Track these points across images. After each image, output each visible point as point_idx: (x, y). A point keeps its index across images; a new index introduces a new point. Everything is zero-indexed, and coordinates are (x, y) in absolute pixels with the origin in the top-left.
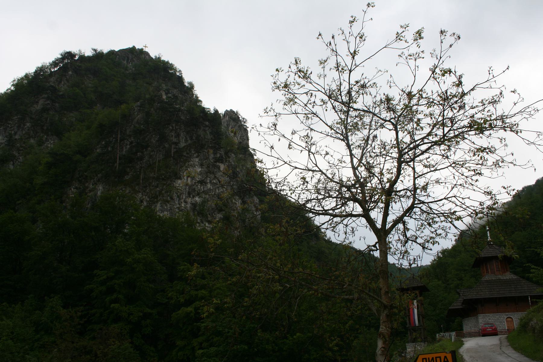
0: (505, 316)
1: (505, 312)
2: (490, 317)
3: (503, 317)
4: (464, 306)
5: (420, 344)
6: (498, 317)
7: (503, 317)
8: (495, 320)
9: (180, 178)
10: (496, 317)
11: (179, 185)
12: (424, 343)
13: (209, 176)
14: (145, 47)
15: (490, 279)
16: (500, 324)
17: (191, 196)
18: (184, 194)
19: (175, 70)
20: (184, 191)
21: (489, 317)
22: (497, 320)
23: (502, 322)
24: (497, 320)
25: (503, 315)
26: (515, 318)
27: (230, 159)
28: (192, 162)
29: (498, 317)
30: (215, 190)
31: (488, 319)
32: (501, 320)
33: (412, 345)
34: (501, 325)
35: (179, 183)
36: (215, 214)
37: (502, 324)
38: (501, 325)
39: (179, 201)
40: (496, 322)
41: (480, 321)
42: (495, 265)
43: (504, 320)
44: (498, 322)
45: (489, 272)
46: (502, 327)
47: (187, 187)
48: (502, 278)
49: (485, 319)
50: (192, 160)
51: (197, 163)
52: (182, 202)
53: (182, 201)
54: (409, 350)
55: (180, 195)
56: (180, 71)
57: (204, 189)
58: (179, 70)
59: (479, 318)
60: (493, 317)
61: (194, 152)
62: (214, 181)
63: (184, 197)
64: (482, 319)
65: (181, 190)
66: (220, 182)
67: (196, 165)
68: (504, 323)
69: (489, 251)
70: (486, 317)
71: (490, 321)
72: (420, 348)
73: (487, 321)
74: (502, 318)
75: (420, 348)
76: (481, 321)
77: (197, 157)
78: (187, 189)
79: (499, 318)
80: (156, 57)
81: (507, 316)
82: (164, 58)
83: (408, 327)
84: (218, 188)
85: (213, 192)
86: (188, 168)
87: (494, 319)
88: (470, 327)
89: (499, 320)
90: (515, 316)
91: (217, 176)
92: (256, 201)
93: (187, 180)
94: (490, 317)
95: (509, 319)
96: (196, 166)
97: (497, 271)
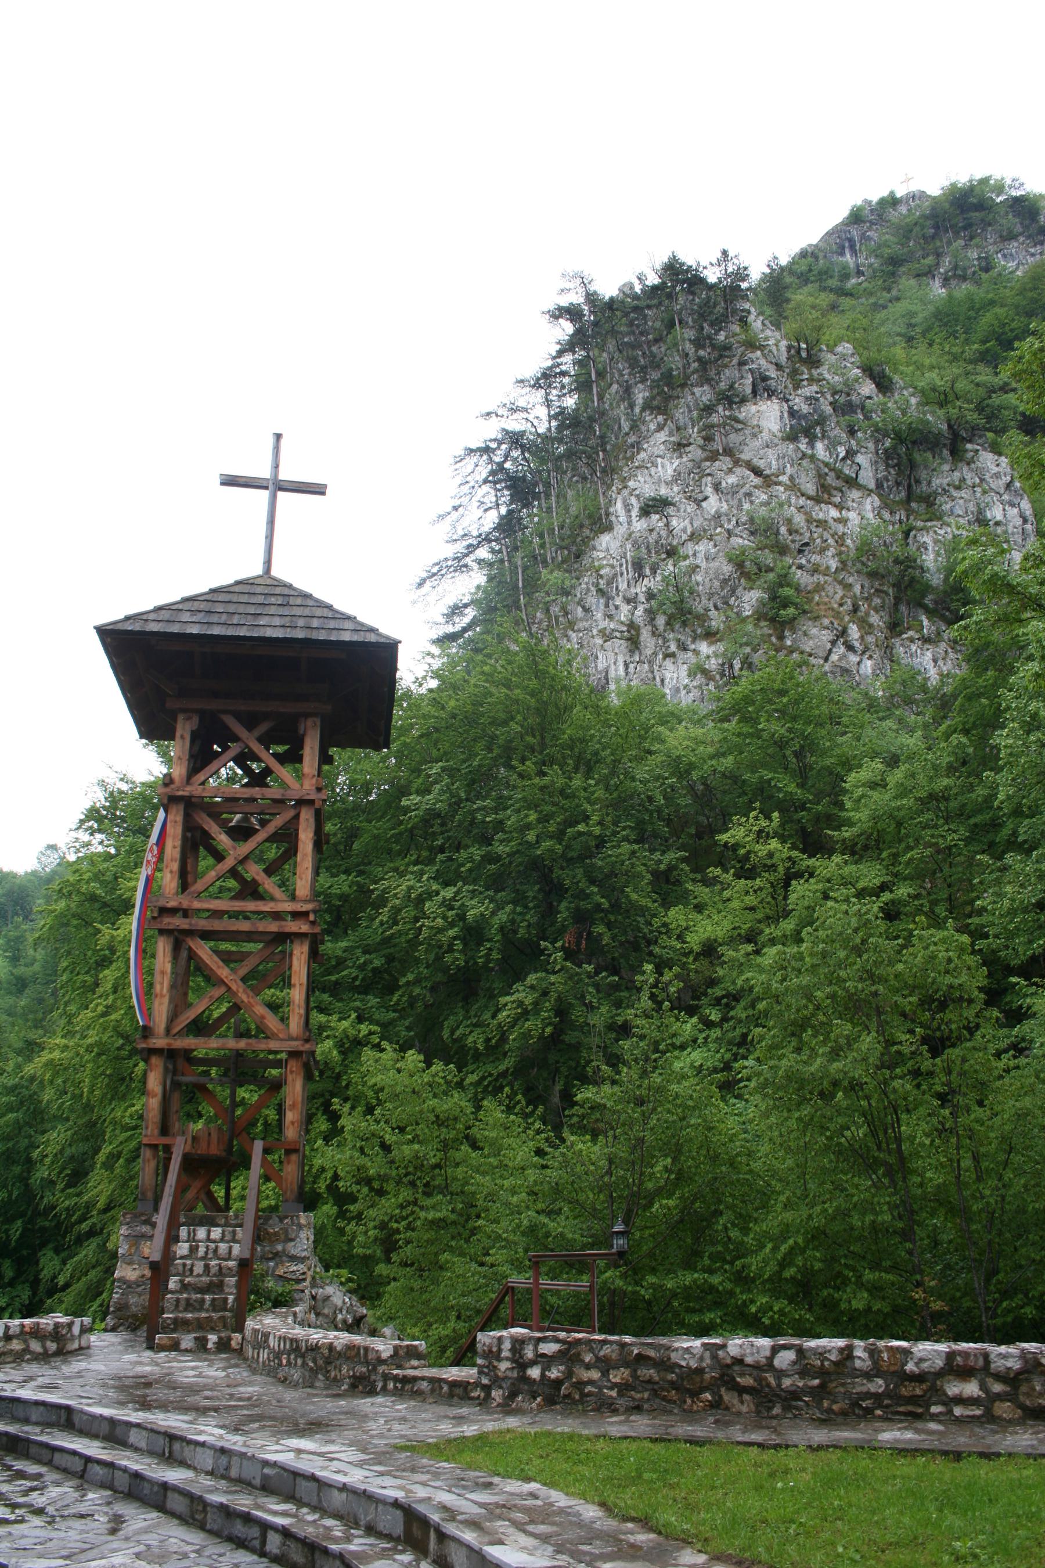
9: (609, 528)
11: (608, 550)
17: (648, 571)
18: (622, 574)
20: (621, 565)
28: (643, 455)
30: (740, 506)
35: (604, 545)
39: (607, 606)
47: (629, 546)
51: (662, 447)
52: (617, 607)
53: (618, 601)
55: (609, 583)
62: (732, 479)
63: (623, 586)
65: (613, 567)
77: (660, 428)
84: (749, 495)
85: (729, 521)
91: (744, 457)
92: (996, 469)
96: (659, 460)
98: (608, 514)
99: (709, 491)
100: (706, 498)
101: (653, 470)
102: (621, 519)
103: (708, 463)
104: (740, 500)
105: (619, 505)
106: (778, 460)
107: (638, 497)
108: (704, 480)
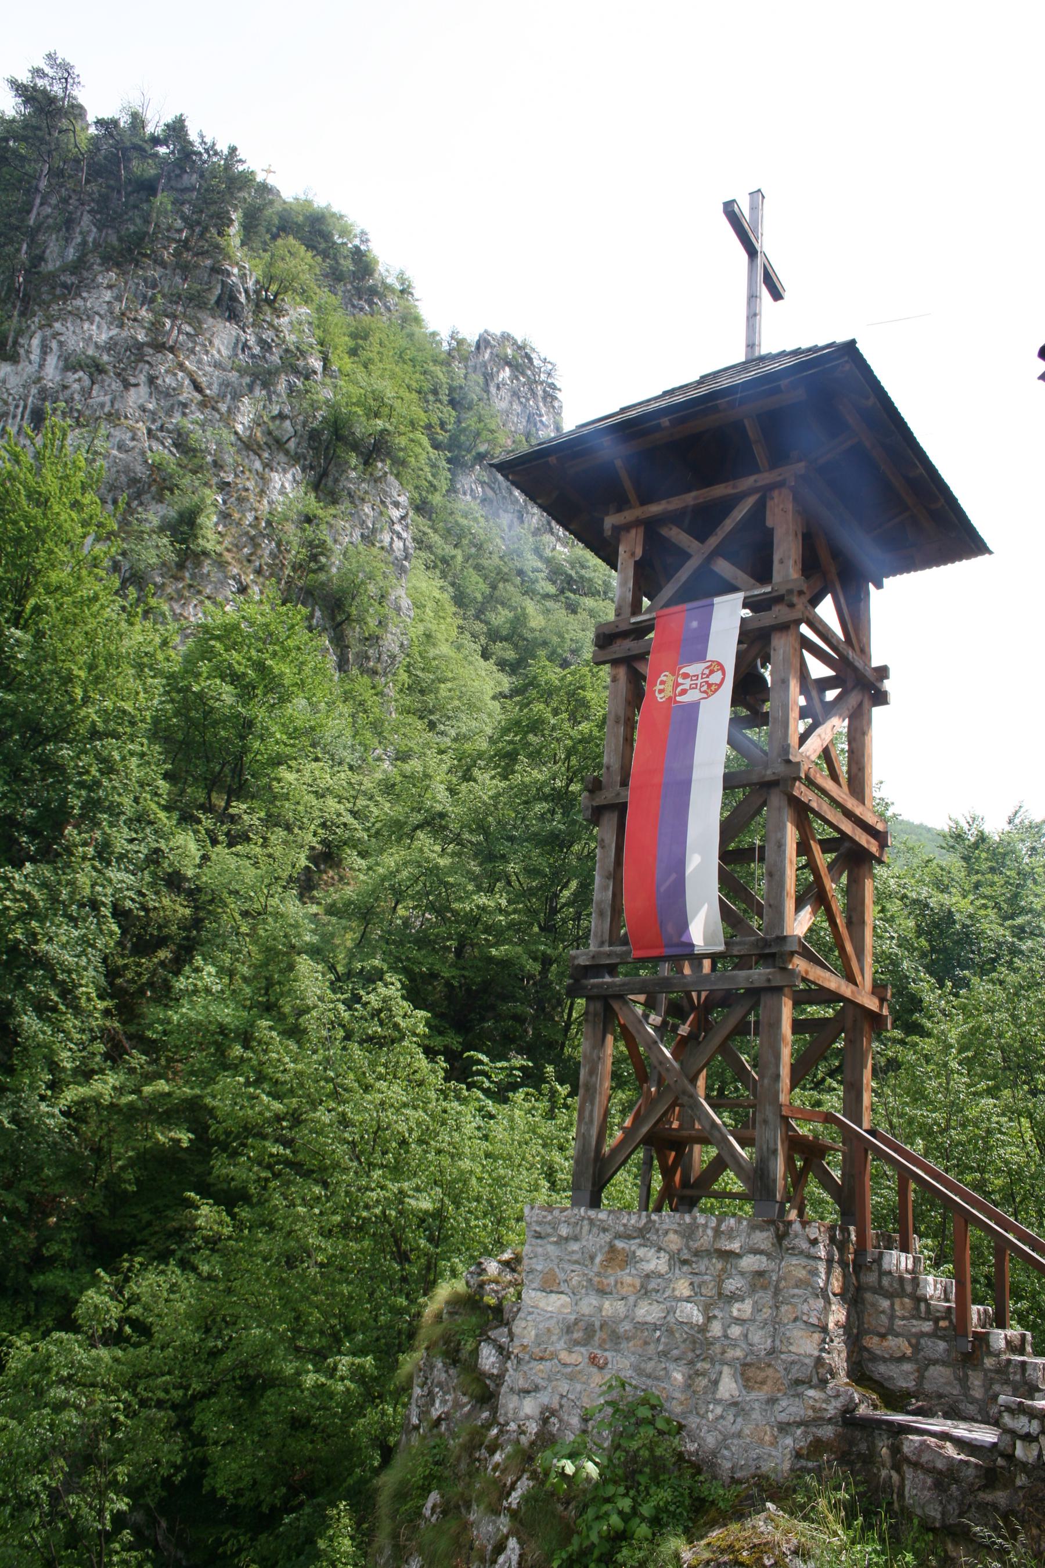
5: (705, 1240)
12: (763, 1239)
13: (147, 358)
14: (269, 171)
18: (14, 417)
19: (345, 232)
20: (17, 407)
27: (284, 320)
28: (79, 302)
36: (141, 504)
47: (34, 391)
50: (85, 294)
54: (555, 1304)
56: (363, 233)
57: (112, 406)
58: (357, 231)
61: (100, 269)
66: (198, 388)
67: (97, 313)
72: (698, 1318)
78: (30, 399)
80: (297, 199)
82: (320, 202)
83: (595, 969)
86: (57, 320)
93: (41, 366)
96: (97, 318)
98: (15, 343)
99: (142, 378)
100: (136, 385)
101: (86, 326)
102: (32, 357)
103: (151, 351)
104: (172, 406)
105: (36, 342)
106: (220, 385)
107: (61, 344)
108: (141, 365)
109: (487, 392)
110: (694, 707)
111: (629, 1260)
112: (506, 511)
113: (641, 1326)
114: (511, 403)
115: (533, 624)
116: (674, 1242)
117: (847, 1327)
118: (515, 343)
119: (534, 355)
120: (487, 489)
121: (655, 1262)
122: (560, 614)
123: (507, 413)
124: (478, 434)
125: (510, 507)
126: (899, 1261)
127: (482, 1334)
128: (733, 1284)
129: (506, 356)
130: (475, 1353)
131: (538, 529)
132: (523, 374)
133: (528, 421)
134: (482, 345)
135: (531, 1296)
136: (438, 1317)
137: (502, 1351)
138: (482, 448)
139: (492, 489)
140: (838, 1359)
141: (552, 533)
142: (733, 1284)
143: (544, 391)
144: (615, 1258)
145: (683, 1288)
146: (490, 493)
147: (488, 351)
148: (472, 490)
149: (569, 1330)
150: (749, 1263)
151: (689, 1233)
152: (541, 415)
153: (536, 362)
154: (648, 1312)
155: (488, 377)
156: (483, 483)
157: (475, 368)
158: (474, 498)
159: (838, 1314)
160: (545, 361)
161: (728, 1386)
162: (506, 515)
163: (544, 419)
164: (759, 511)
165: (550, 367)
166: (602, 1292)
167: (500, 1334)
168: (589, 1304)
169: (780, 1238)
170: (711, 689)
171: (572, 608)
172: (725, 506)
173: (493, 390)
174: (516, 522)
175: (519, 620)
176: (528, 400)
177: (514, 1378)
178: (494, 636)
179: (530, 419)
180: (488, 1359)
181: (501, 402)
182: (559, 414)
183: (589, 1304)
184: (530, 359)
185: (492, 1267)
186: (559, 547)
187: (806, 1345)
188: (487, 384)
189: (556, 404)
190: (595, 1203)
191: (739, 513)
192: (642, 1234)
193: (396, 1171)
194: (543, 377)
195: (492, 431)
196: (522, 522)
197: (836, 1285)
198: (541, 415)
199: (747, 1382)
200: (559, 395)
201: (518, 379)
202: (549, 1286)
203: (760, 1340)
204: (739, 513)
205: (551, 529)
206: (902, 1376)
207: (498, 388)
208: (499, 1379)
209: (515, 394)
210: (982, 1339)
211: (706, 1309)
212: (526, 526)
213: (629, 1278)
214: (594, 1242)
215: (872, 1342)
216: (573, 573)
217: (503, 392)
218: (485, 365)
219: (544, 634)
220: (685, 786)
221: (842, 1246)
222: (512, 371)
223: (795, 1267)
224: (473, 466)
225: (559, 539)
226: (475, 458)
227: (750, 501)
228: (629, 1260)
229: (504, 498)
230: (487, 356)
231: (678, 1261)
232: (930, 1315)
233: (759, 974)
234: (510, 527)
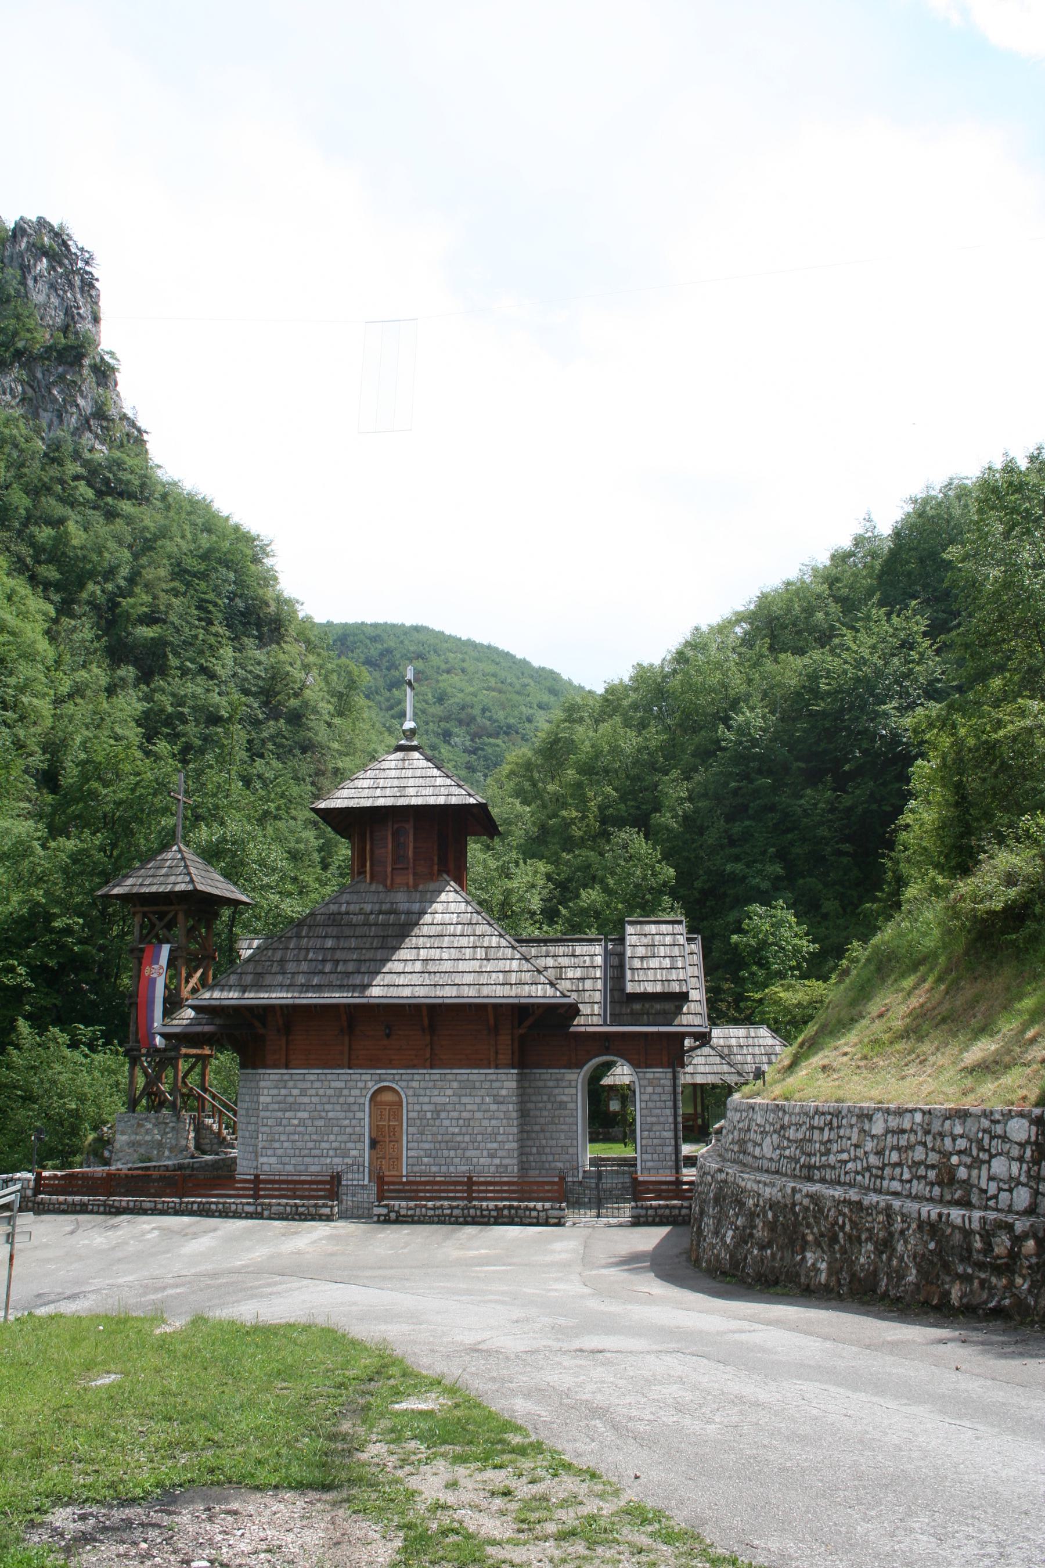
0: (370, 1084)
1: (373, 1062)
2: (309, 1085)
3: (360, 1085)
4: (218, 1021)
5: (161, 1120)
6: (342, 1085)
7: (360, 1085)
8: (324, 1100)
10: (333, 1084)
12: (174, 1119)
15: (352, 908)
16: (342, 1115)
21: (300, 1084)
22: (334, 1100)
23: (355, 1108)
24: (334, 1100)
25: (364, 1077)
26: (410, 1092)
29: (342, 1085)
31: (295, 1092)
32: (351, 1100)
33: (134, 1122)
34: (347, 1122)
37: (351, 1115)
38: (347, 1122)
40: (328, 1107)
41: (262, 1099)
42: (390, 846)
43: (362, 1101)
44: (338, 1107)
45: (365, 872)
46: (349, 1130)
48: (403, 907)
49: (283, 1092)
54: (124, 1138)
59: (262, 1084)
60: (317, 1084)
64: (275, 1092)
68: (359, 1115)
69: (382, 783)
70: (291, 1084)
71: (306, 1100)
72: (159, 1137)
73: (291, 1099)
74: (356, 1092)
75: (159, 1137)
76: (268, 1099)
79: (345, 1092)
81: (377, 1082)
87: (321, 1092)
88: (247, 1109)
89: (342, 1100)
90: (415, 1084)
94: (309, 1085)
95: (388, 1097)
97: (393, 869)
109: (23, 283)
110: (155, 979)
111: (143, 1126)
112: (45, 410)
113: (147, 1141)
114: (48, 296)
115: (75, 542)
116: (153, 1121)
117: (195, 1138)
118: (51, 229)
119: (70, 243)
120: (27, 388)
121: (149, 1126)
122: (101, 528)
123: (46, 306)
124: (15, 333)
125: (49, 406)
126: (209, 1121)
127: (104, 1148)
128: (168, 1130)
129: (43, 246)
130: (103, 1153)
131: (77, 429)
132: (61, 265)
133: (66, 314)
134: (18, 234)
135: (118, 1137)
136: (90, 1145)
137: (111, 1152)
138: (20, 345)
139: (32, 387)
140: (192, 1145)
141: (91, 431)
142: (168, 1130)
143: (82, 280)
144: (140, 1125)
145: (156, 1132)
146: (30, 392)
147: (25, 240)
148: (11, 389)
149: (128, 1144)
150: (171, 1125)
151: (157, 1118)
152: (78, 308)
153: (74, 250)
154: (148, 1138)
155: (25, 269)
156: (22, 382)
157: (11, 257)
158: (14, 397)
159: (192, 1135)
160: (82, 249)
161: (167, 1153)
162: (45, 414)
163: (81, 311)
164: (176, 915)
165: (87, 255)
166: (137, 1134)
167: (110, 1147)
168: (133, 1137)
169: (178, 1118)
170: (160, 974)
171: (111, 515)
172: (166, 913)
173: (30, 283)
174: (56, 421)
175: (62, 539)
176: (65, 292)
177: (114, 1157)
178: (38, 549)
179: (68, 312)
180: (106, 1154)
181: (39, 295)
182: (96, 303)
183: (133, 1137)
184: (67, 247)
185: (105, 1129)
186: (98, 446)
187: (184, 1142)
188: (24, 277)
189: (93, 293)
190: (134, 1111)
191: (170, 916)
192: (146, 1119)
193: (61, 1097)
194: (80, 264)
195: (28, 330)
196: (61, 421)
197: (192, 1128)
198: (78, 308)
199: (171, 1152)
200: (97, 284)
201: (55, 270)
202: (123, 1133)
203: (174, 1142)
204: (170, 916)
205: (90, 426)
206: (207, 1148)
207: (36, 281)
208: (110, 1159)
209: (53, 286)
210: (224, 1138)
211: (162, 1136)
212: (65, 428)
213: (143, 1130)
214: (134, 1122)
215: (201, 1141)
216: (111, 476)
217: (40, 285)
218: (21, 255)
219: (85, 552)
220: (153, 1002)
221: (194, 1119)
222: (49, 261)
223: (181, 1125)
224: (12, 364)
225: (97, 437)
226: (14, 356)
227: (173, 913)
228: (143, 1126)
229: (43, 396)
230: (23, 245)
231: (155, 1125)
232: (214, 1133)
233: (173, 1054)
234: (50, 426)
